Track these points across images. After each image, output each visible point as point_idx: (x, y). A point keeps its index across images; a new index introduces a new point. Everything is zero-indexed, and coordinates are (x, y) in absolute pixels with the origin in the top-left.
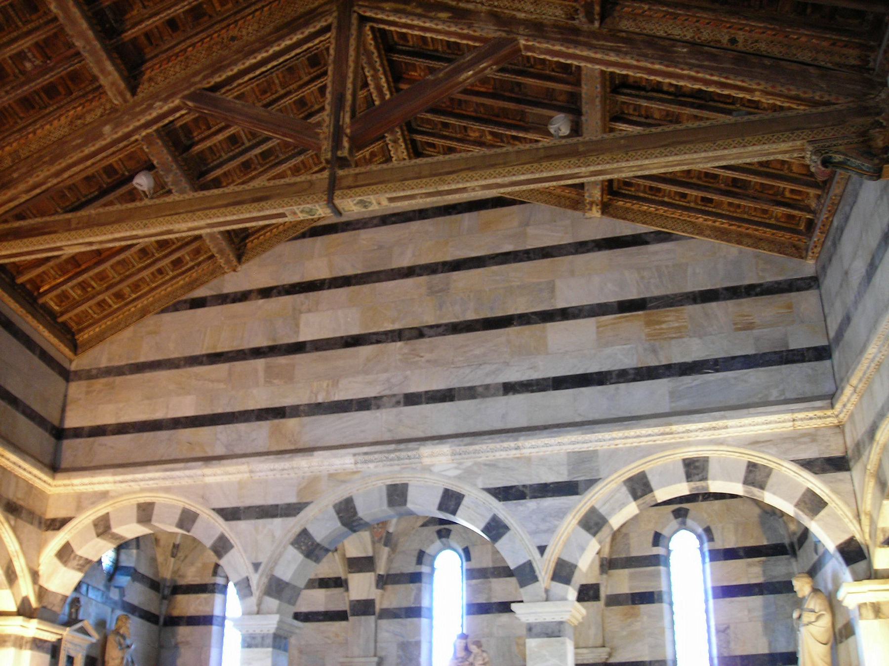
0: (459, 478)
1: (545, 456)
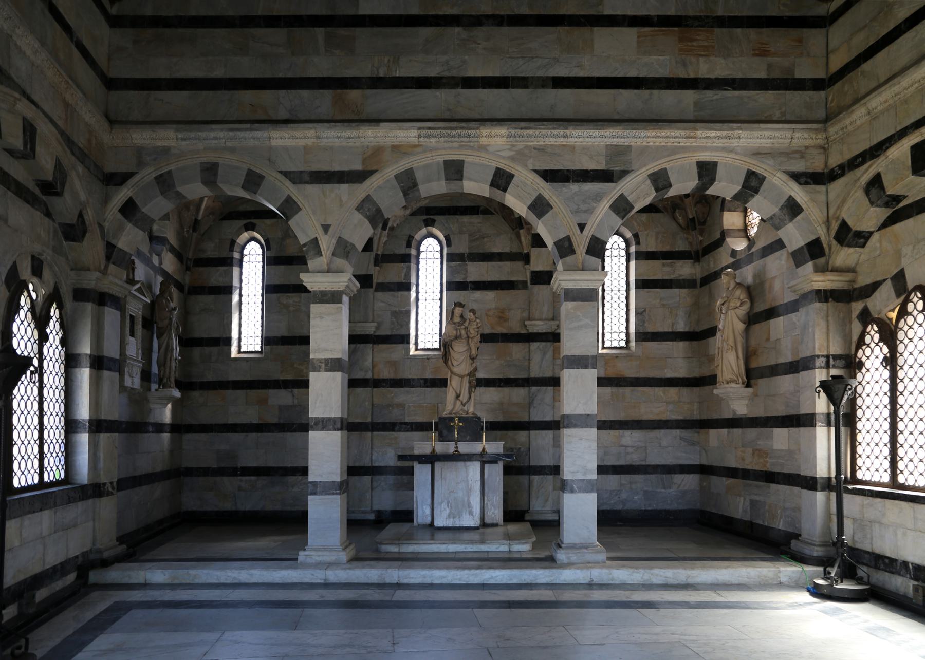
0: (512, 159)
1: (587, 144)
